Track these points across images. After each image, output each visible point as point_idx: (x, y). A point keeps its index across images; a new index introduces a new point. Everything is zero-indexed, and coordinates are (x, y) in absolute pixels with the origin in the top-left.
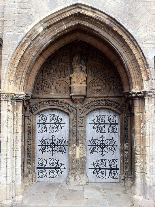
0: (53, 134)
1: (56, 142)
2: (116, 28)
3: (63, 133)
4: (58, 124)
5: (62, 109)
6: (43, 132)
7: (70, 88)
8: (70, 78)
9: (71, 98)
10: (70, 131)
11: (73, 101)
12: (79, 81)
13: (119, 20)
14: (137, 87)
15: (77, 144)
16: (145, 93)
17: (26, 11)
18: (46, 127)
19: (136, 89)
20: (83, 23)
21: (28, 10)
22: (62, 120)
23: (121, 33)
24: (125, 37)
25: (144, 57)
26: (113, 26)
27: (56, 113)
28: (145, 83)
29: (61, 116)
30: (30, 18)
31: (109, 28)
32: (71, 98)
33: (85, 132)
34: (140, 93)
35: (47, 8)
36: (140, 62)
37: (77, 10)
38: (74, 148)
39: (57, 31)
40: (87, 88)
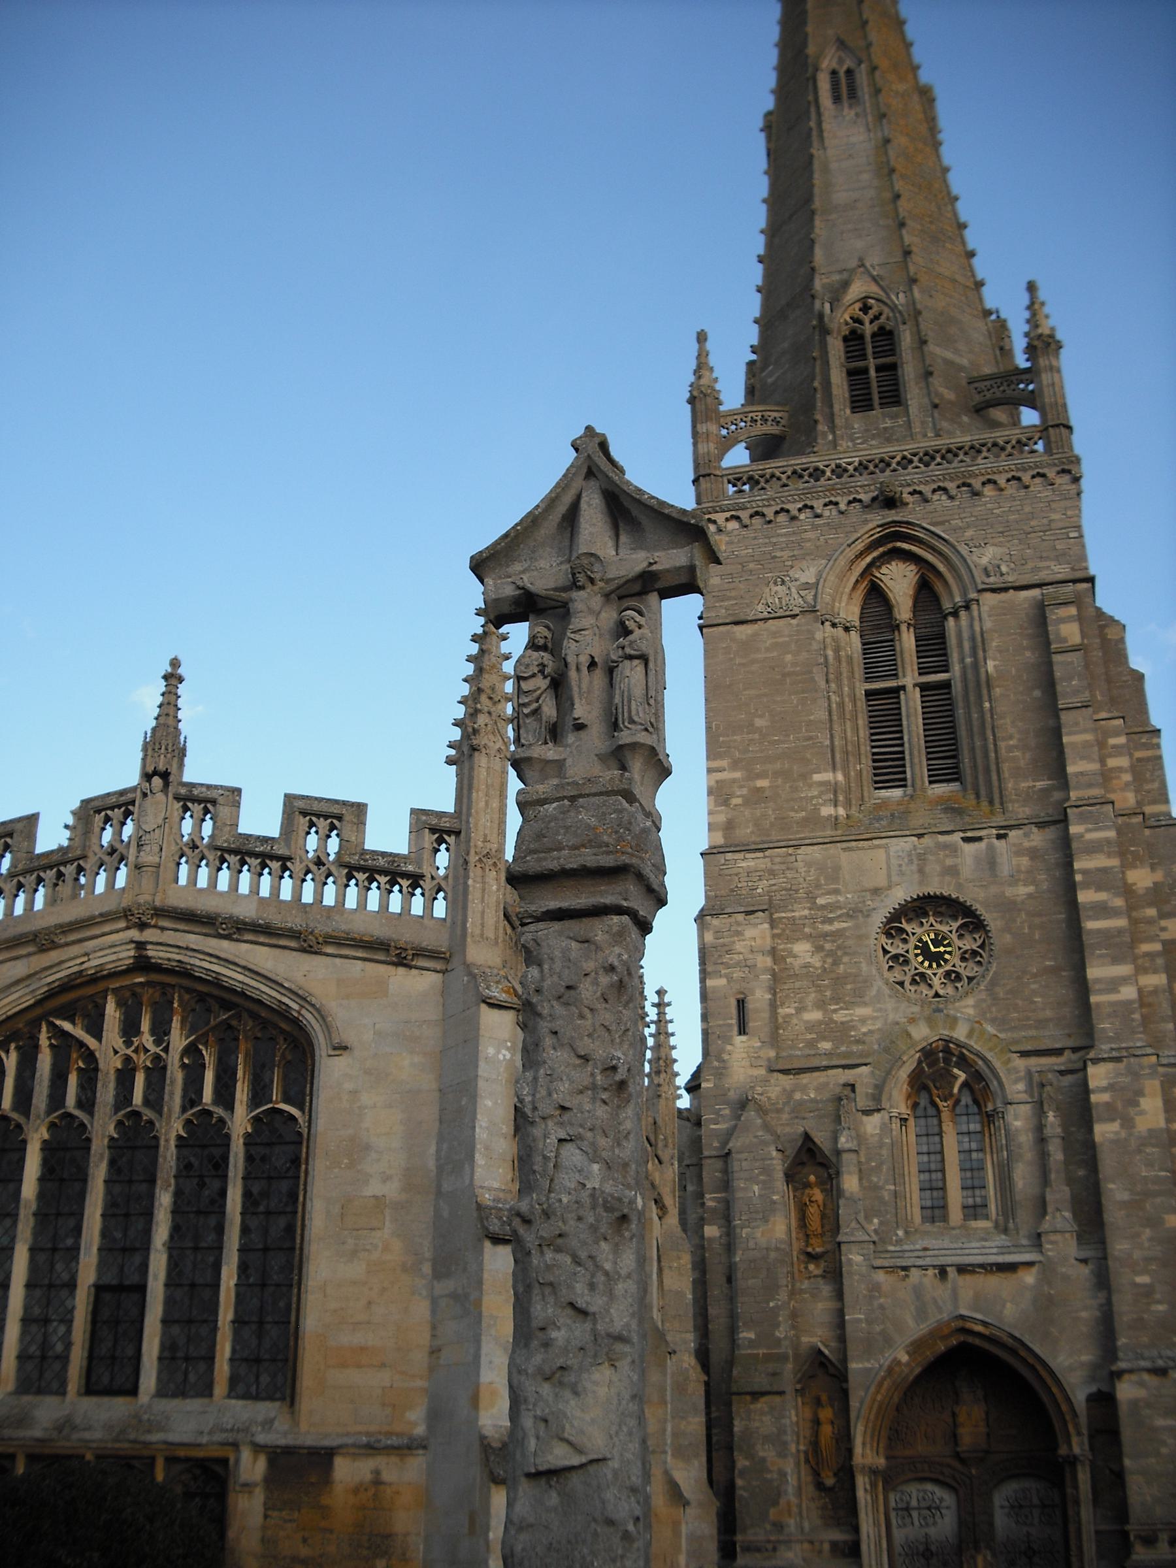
0: (927, 1530)
1: (933, 1548)
2: (1023, 1353)
3: (945, 1526)
4: (933, 1508)
5: (941, 1478)
6: (905, 1525)
7: (955, 1435)
8: (954, 1415)
9: (957, 1456)
10: (961, 1523)
11: (962, 1461)
12: (972, 1419)
13: (1027, 1339)
14: (1065, 1446)
15: (977, 1549)
16: (1075, 1457)
17: (878, 1328)
18: (910, 1516)
19: (1063, 1451)
20: (970, 1339)
21: (882, 1327)
22: (941, 1500)
23: (1031, 1360)
24: (1039, 1368)
25: (1068, 1399)
26: (1017, 1347)
27: (929, 1487)
28: (1075, 1440)
29: (939, 1492)
30: (888, 1341)
31: (1013, 1351)
32: (957, 1456)
33: (991, 1524)
34: (1068, 1456)
35: (911, 1323)
36: (1064, 1407)
37: (960, 1324)
38: (974, 1558)
39: (930, 1355)
40: (988, 1435)
